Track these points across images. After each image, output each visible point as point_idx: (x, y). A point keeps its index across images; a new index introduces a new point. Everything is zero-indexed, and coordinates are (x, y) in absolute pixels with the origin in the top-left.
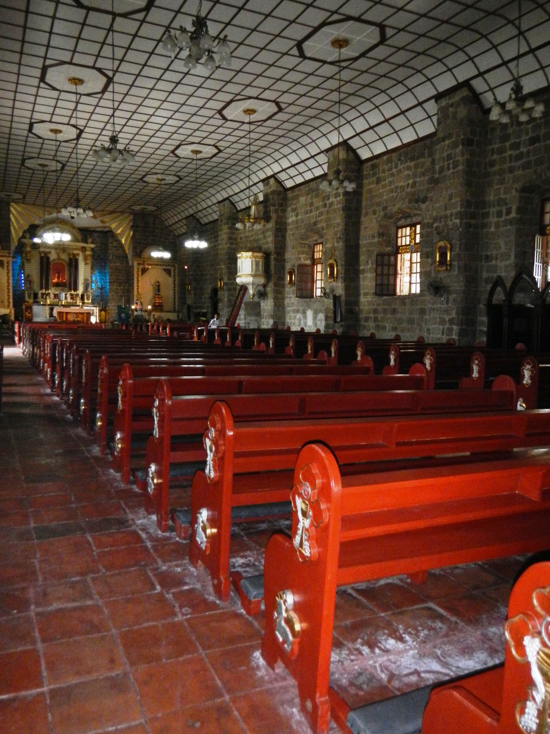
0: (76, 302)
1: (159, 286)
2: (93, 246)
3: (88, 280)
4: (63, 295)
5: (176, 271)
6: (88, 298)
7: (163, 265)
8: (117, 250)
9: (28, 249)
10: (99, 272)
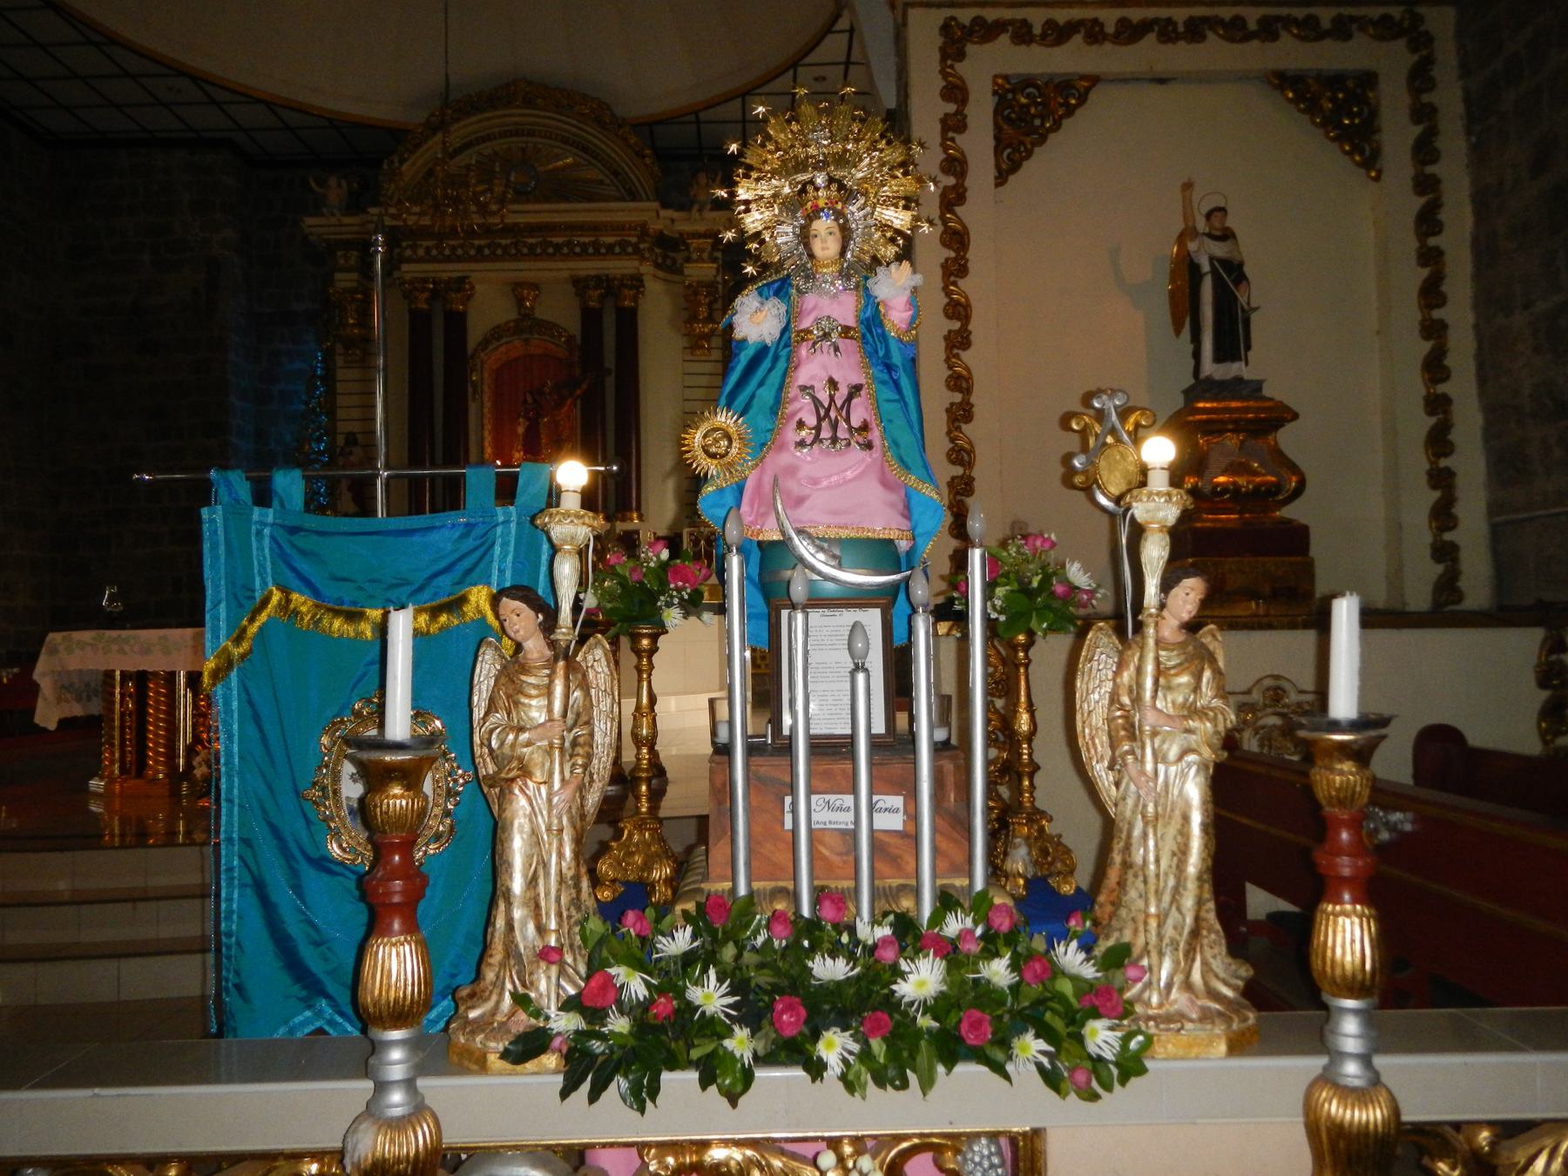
1: (1232, 272)
5: (1449, 98)
7: (1268, 31)
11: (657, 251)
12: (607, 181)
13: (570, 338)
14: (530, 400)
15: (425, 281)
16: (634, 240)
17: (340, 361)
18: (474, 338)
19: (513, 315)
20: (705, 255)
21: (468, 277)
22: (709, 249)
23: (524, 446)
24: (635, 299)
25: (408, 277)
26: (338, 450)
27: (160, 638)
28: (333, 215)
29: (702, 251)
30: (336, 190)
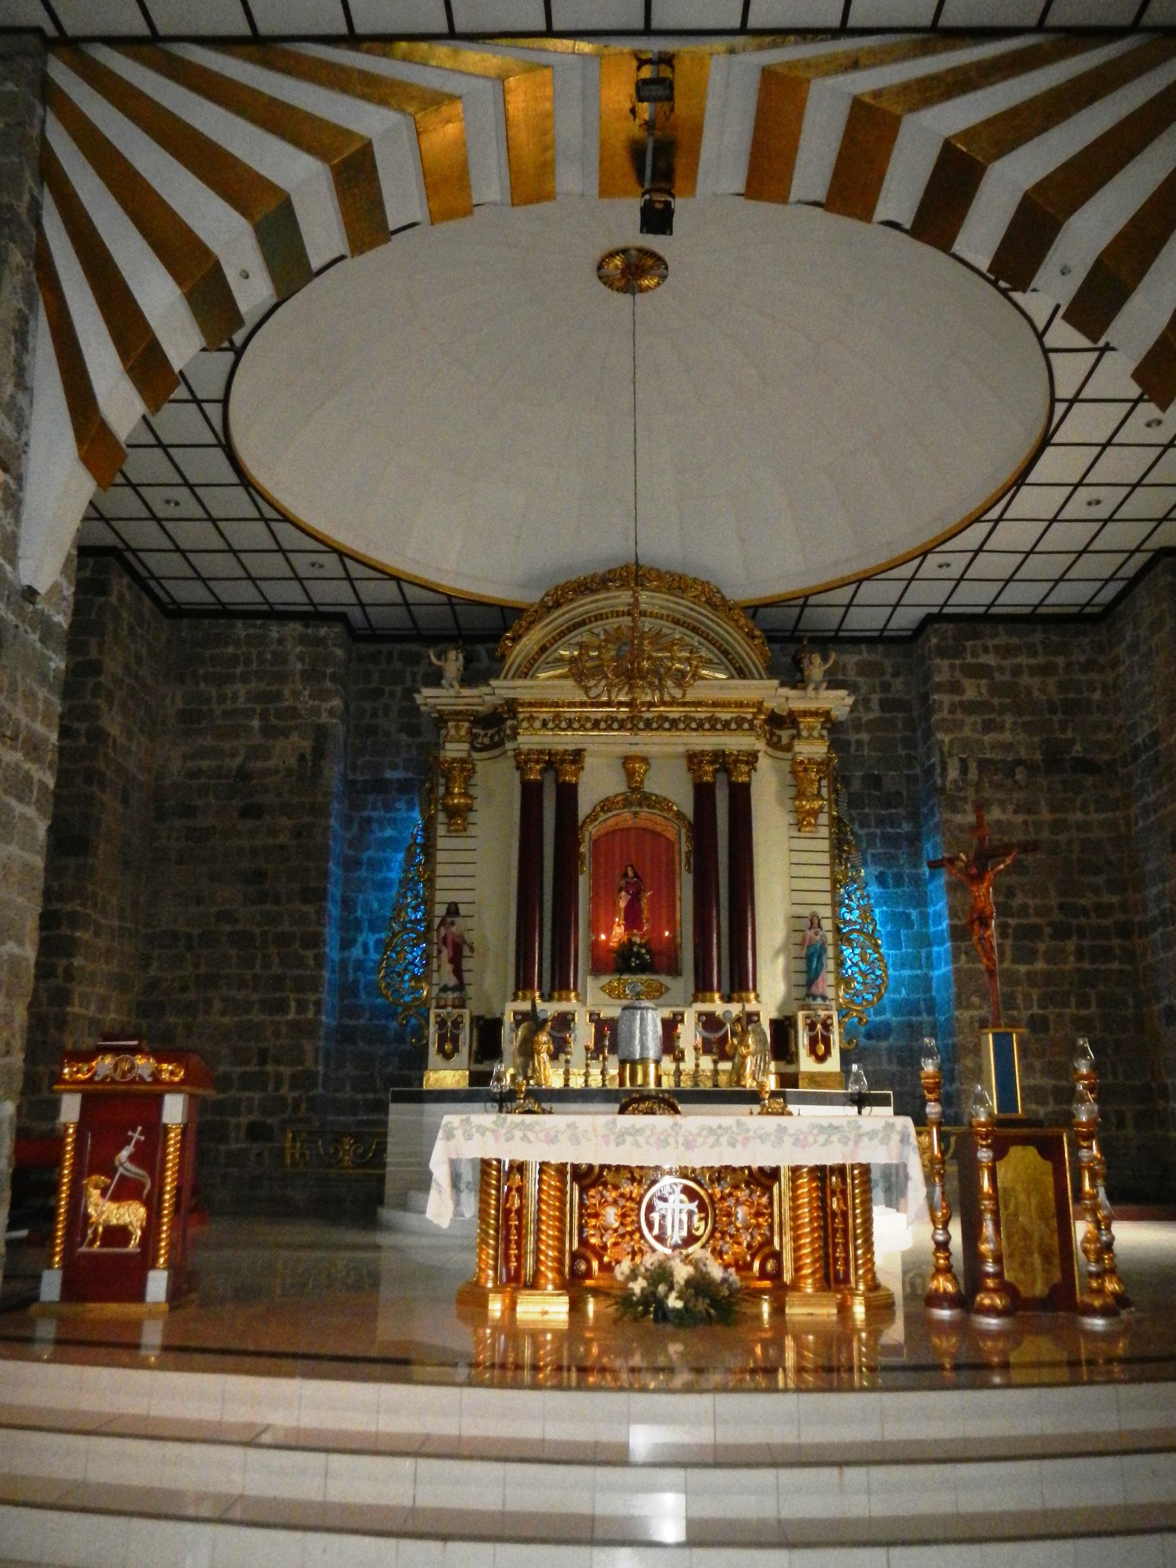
0: (738, 1072)
2: (838, 702)
3: (814, 922)
4: (652, 1020)
6: (819, 1047)
8: (988, 727)
9: (454, 750)
10: (881, 880)
11: (767, 728)
12: (716, 660)
13: (680, 815)
14: (630, 873)
15: (541, 752)
16: (749, 717)
17: (441, 830)
18: (584, 810)
19: (622, 788)
20: (816, 734)
21: (584, 750)
22: (819, 727)
23: (626, 919)
24: (749, 773)
25: (525, 748)
26: (437, 921)
27: (568, 1126)
28: (452, 686)
29: (811, 729)
30: (453, 663)
